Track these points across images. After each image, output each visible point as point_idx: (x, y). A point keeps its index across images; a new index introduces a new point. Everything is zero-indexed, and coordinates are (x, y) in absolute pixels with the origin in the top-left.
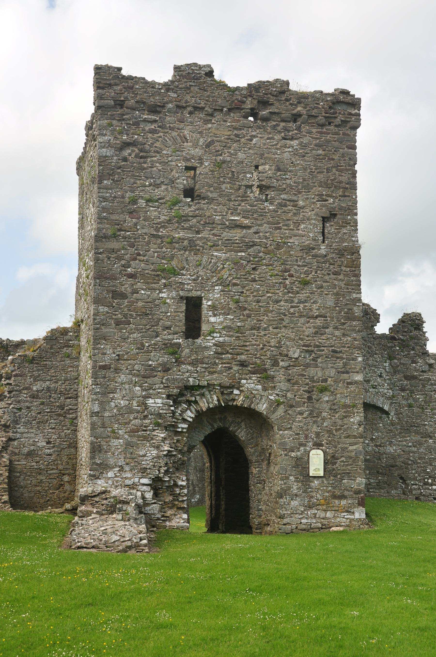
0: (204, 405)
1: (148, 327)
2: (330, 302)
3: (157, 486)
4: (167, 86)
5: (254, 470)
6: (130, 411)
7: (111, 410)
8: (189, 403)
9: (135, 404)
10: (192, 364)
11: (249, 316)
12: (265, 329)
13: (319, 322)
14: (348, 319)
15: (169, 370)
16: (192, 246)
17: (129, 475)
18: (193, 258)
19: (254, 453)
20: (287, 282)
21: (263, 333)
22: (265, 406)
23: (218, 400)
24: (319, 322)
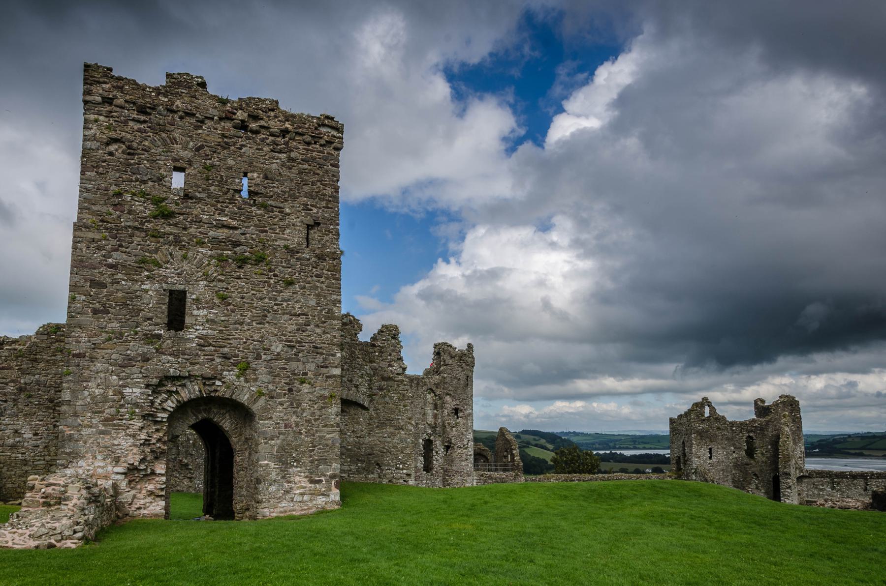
1: (128, 317)
2: (313, 302)
5: (238, 459)
6: (105, 400)
7: (84, 399)
8: (170, 393)
9: (111, 392)
11: (233, 311)
12: (249, 324)
14: (328, 318)
15: (148, 360)
16: (177, 242)
17: (101, 464)
18: (179, 254)
19: (238, 442)
20: (272, 281)
21: (246, 328)
22: (246, 397)
23: (200, 391)
24: (301, 320)
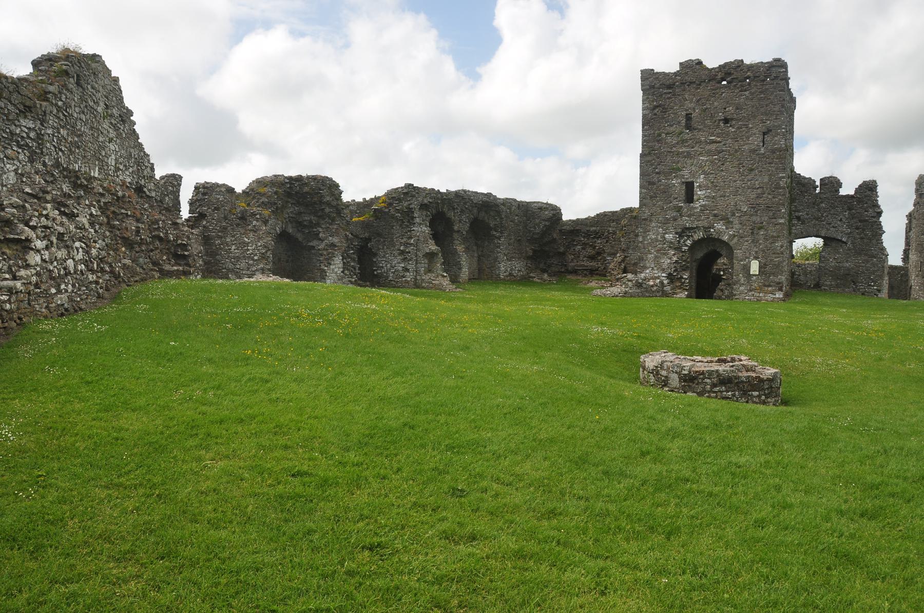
0: (696, 237)
2: (766, 180)
3: (670, 276)
4: (676, 74)
6: (657, 240)
10: (688, 216)
13: (759, 191)
16: (689, 155)
24: (759, 191)
